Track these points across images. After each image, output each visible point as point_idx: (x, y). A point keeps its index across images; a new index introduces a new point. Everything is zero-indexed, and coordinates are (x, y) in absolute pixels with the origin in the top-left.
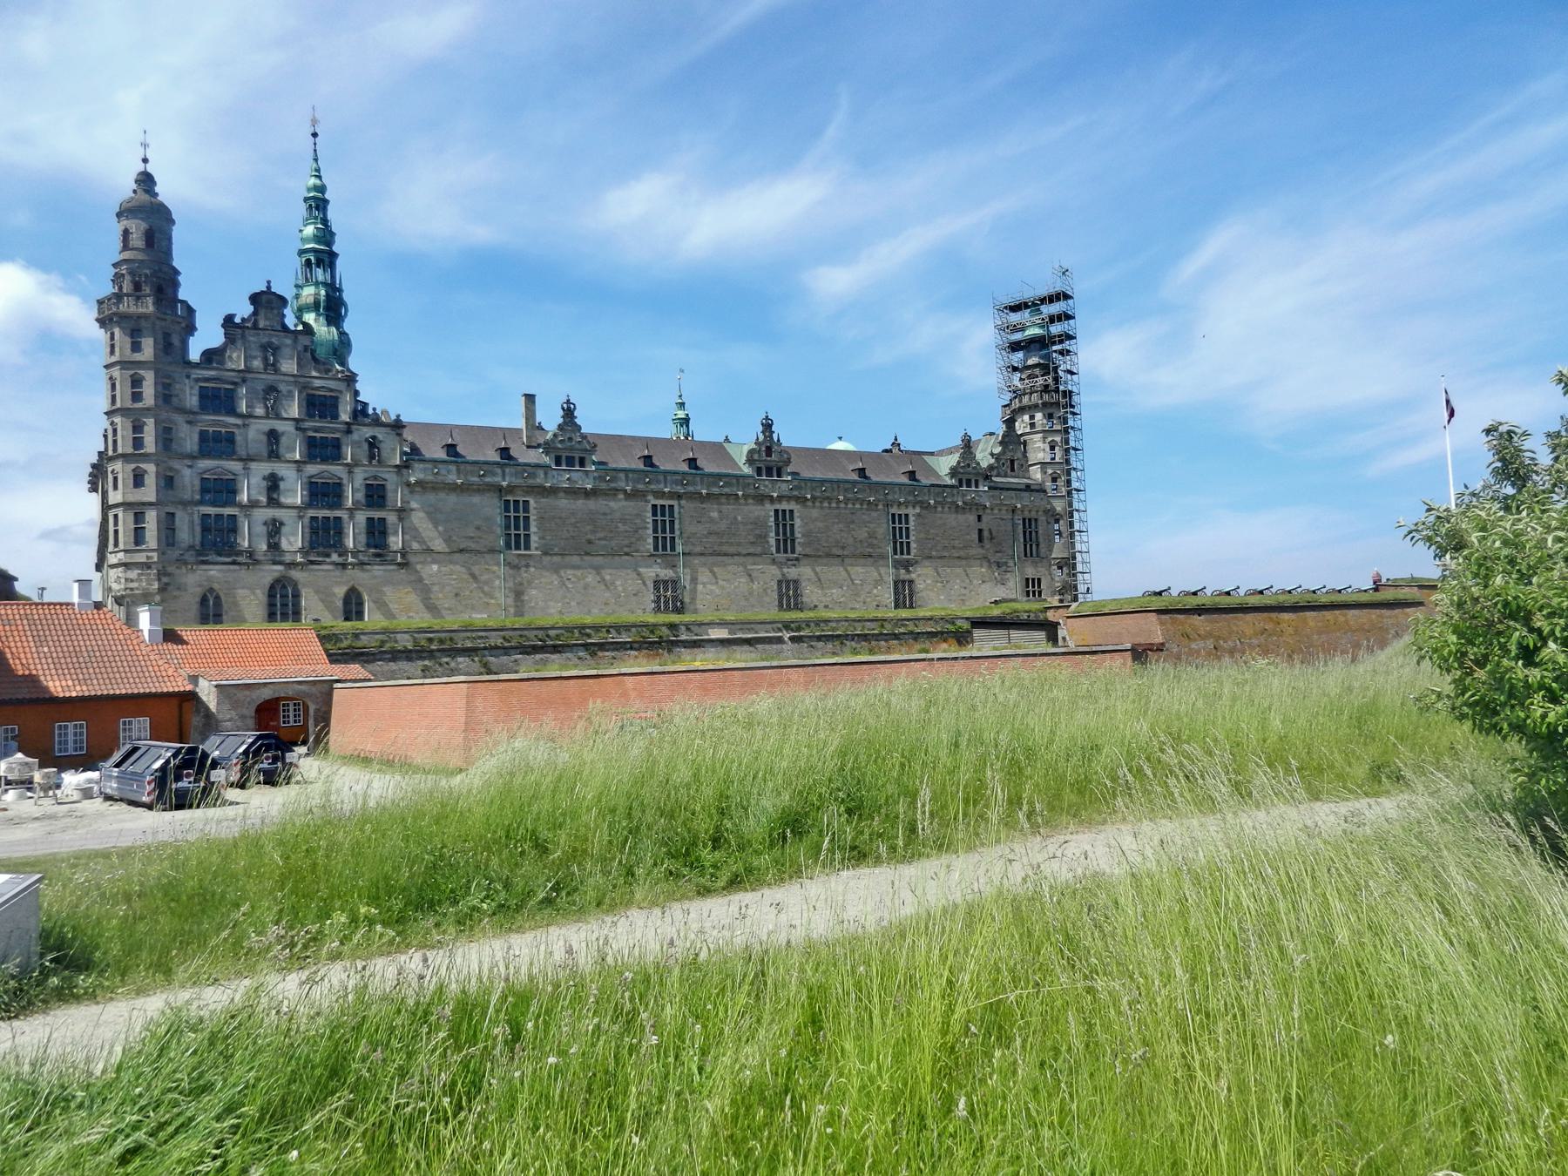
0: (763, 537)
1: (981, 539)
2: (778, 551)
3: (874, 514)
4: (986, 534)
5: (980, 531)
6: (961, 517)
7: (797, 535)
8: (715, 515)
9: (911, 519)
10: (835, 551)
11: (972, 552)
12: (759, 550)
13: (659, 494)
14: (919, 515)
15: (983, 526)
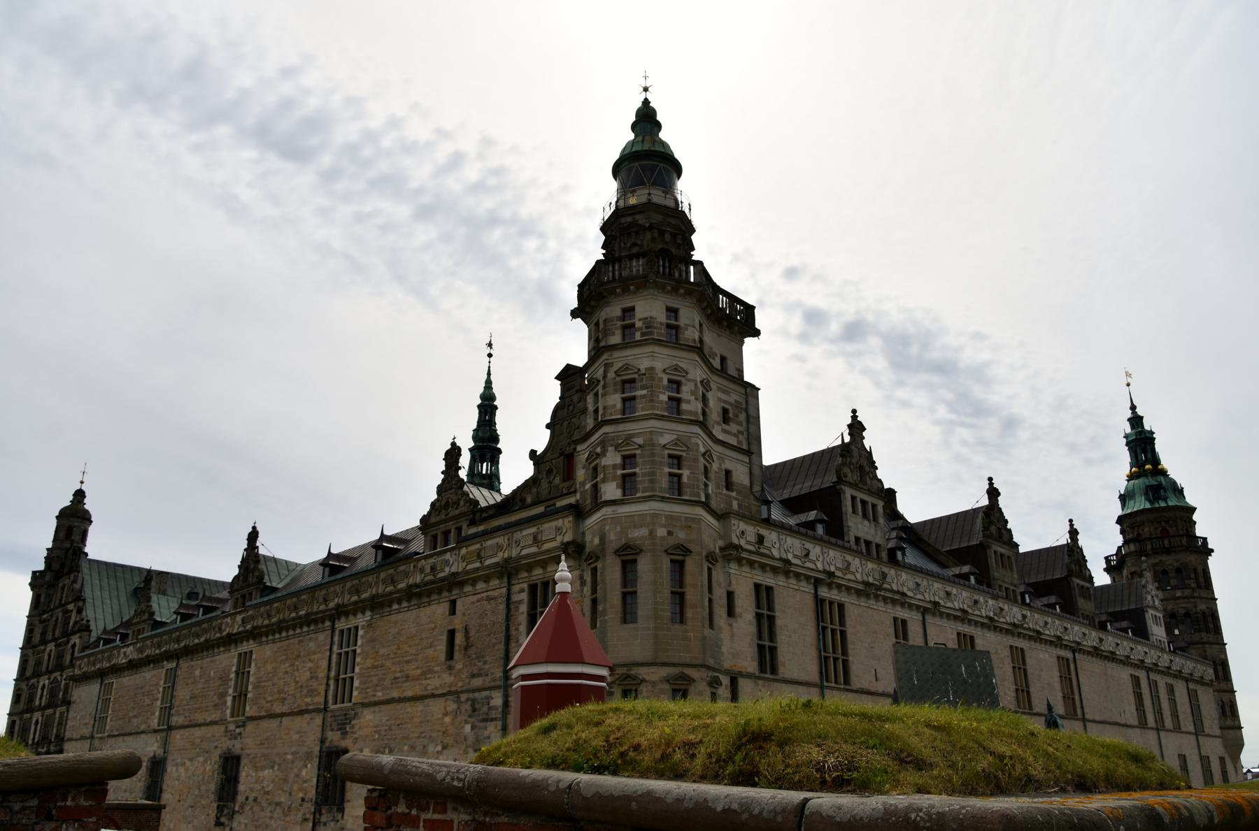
0: (223, 695)
1: (450, 655)
2: (232, 716)
3: (321, 637)
4: (459, 639)
5: (452, 634)
6: (425, 613)
7: (250, 688)
8: (197, 673)
9: (361, 632)
10: (278, 709)
11: (434, 683)
12: (216, 716)
13: (169, 656)
14: (370, 625)
15: (458, 623)
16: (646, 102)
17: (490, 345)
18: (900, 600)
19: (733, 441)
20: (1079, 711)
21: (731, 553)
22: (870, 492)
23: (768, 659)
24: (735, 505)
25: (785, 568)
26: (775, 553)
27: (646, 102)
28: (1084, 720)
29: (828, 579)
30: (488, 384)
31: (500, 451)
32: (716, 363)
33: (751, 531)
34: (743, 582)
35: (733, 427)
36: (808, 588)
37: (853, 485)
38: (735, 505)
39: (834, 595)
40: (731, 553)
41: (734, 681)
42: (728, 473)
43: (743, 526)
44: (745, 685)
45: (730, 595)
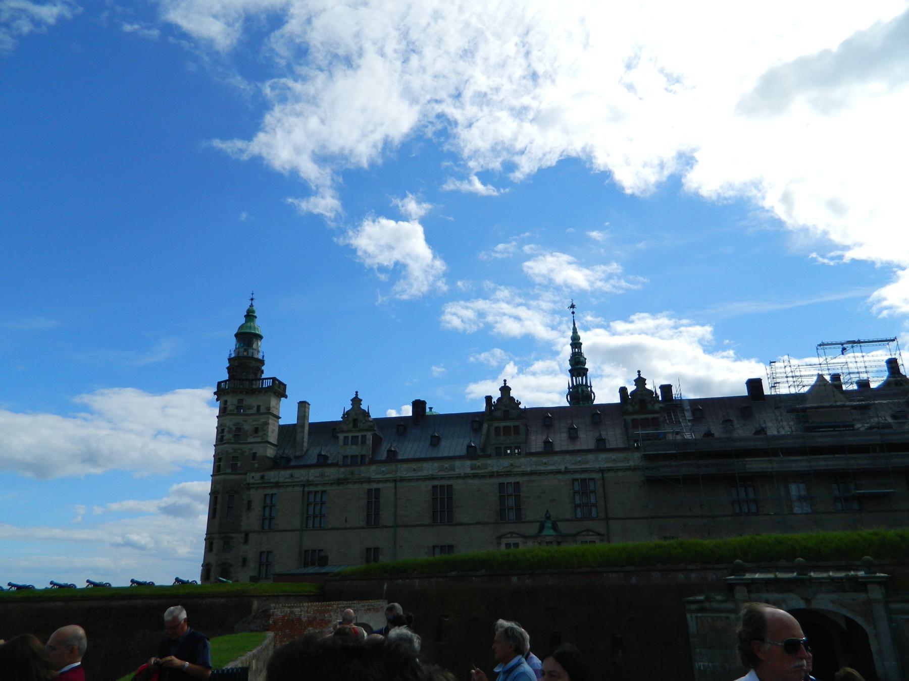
16: (251, 306)
17: (573, 306)
18: (370, 481)
19: (259, 440)
21: (249, 487)
22: (360, 430)
23: (268, 523)
24: (256, 465)
25: (277, 485)
26: (272, 480)
27: (251, 306)
28: (607, 518)
29: (308, 483)
30: (575, 330)
31: (587, 370)
32: (254, 410)
33: (257, 476)
34: (256, 496)
35: (260, 434)
36: (298, 489)
37: (343, 432)
38: (256, 465)
39: (320, 488)
40: (249, 487)
41: (247, 535)
42: (255, 454)
43: (253, 474)
44: (253, 537)
45: (249, 502)
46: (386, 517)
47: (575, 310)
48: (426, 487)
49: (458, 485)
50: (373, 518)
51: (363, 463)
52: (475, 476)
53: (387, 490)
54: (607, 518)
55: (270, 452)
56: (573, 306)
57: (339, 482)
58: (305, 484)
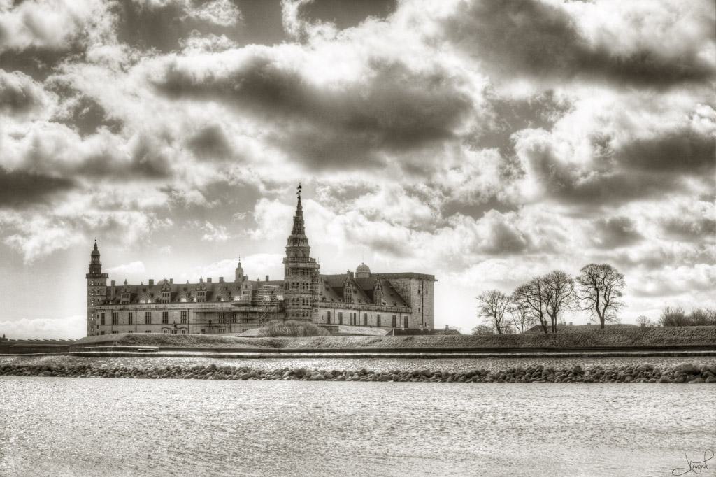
17: (300, 187)
18: (128, 310)
20: (187, 322)
23: (103, 323)
25: (104, 310)
28: (189, 324)
46: (134, 322)
47: (301, 190)
48: (144, 312)
49: (152, 312)
50: (130, 323)
51: (128, 304)
52: (156, 309)
53: (134, 312)
54: (189, 324)
55: (104, 298)
56: (300, 187)
57: (121, 310)
58: (112, 310)
